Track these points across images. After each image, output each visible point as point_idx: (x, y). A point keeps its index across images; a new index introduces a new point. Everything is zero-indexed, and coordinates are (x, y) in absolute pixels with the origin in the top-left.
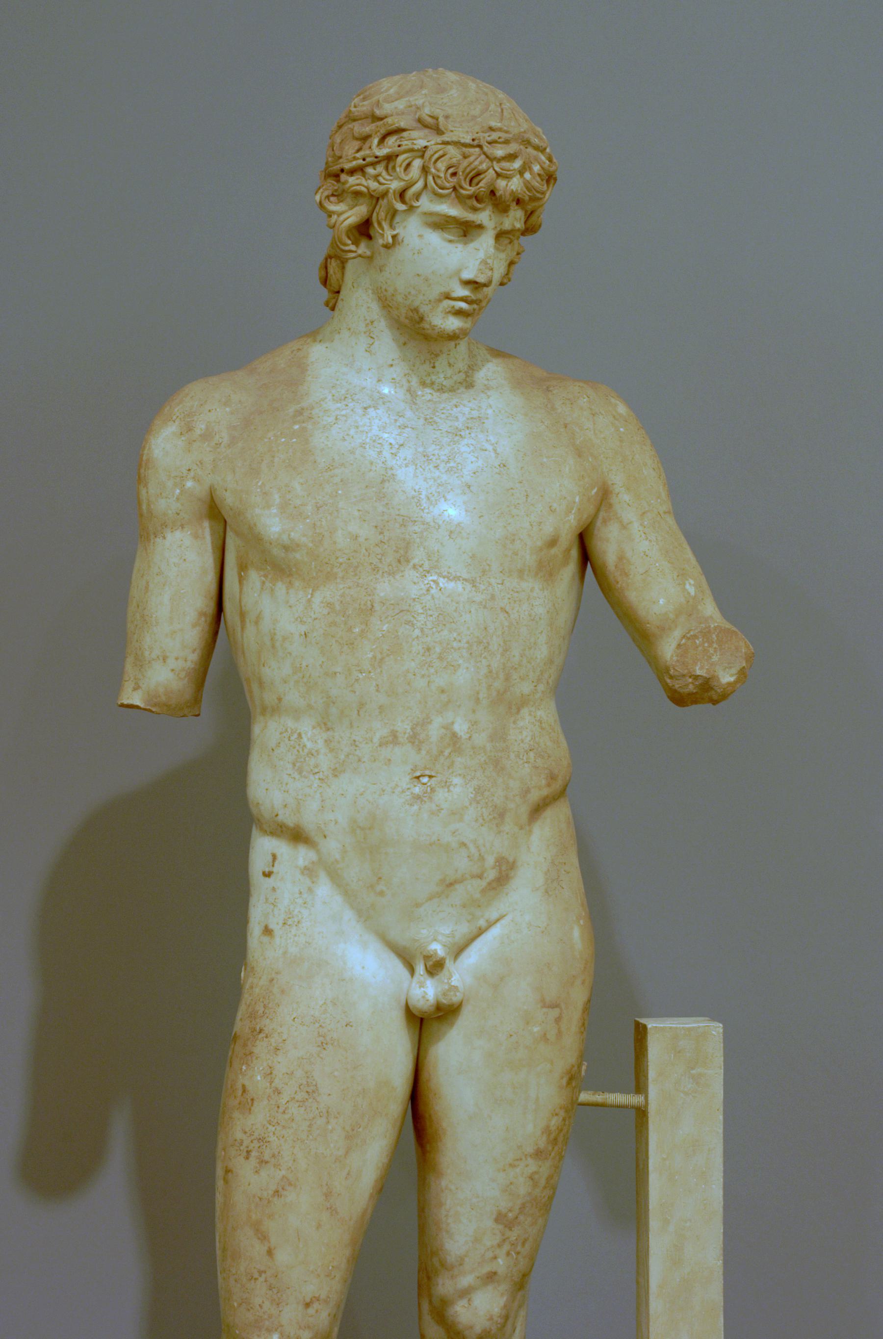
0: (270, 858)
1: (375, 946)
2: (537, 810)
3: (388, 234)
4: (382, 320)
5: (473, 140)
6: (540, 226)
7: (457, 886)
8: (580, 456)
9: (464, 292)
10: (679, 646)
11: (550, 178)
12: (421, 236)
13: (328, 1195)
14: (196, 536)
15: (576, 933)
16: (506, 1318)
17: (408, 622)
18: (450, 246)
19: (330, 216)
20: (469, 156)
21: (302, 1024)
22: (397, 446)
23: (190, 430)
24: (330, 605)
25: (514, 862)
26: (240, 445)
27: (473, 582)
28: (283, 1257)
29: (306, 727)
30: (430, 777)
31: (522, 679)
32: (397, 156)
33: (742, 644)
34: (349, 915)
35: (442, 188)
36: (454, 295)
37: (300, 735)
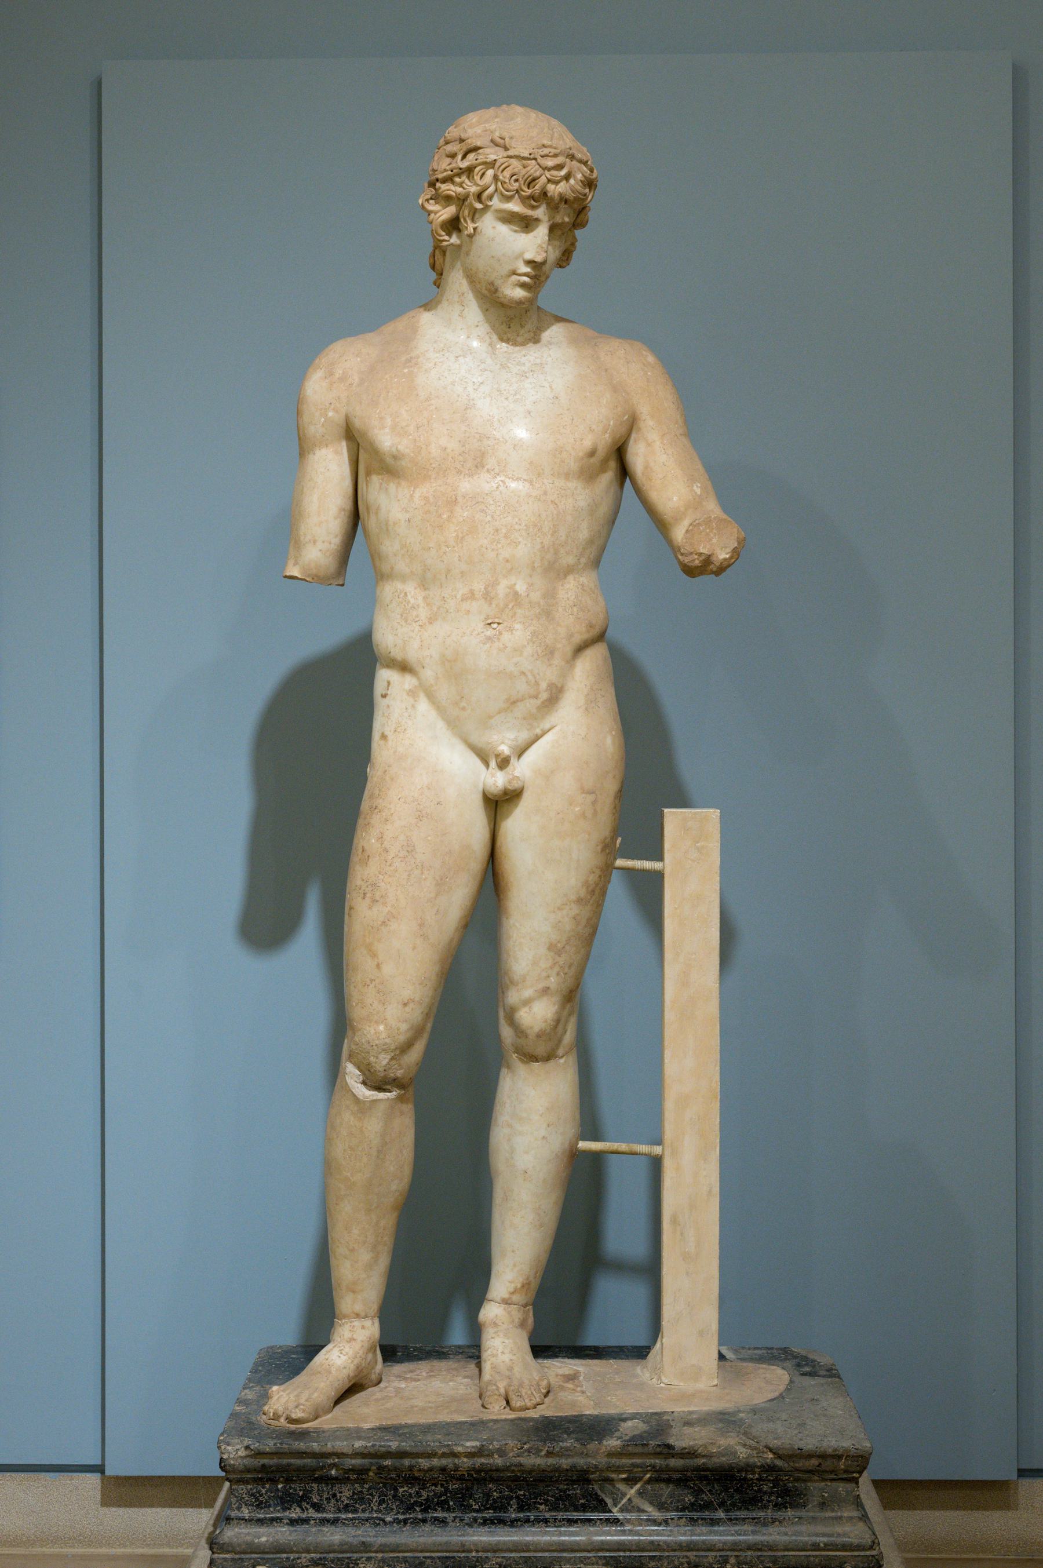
0: (386, 684)
1: (461, 748)
2: (580, 649)
3: (471, 226)
7: (519, 704)
8: (615, 392)
9: (528, 270)
10: (687, 531)
12: (494, 228)
13: (421, 925)
14: (336, 452)
15: (609, 741)
16: (558, 1021)
17: (482, 511)
21: (405, 802)
23: (332, 374)
24: (426, 498)
25: (562, 687)
27: (531, 482)
28: (388, 969)
29: (411, 589)
30: (499, 624)
31: (567, 553)
33: (735, 530)
34: (441, 724)
36: (519, 271)
37: (406, 594)
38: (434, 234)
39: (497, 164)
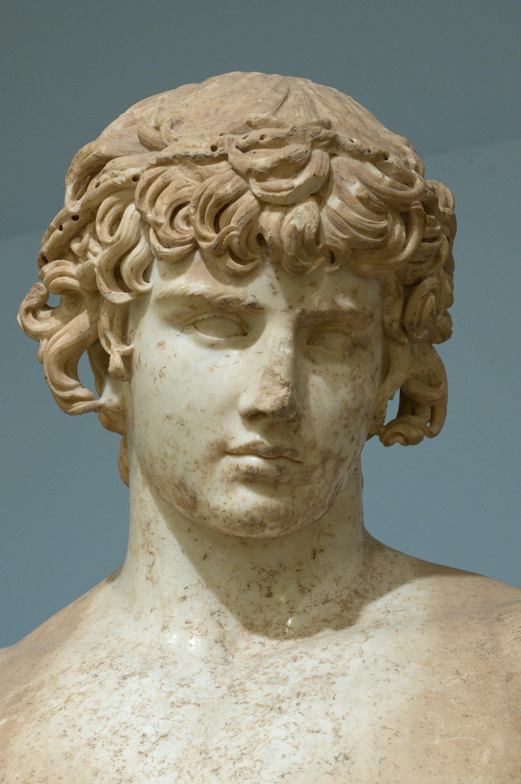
4: (161, 518)
5: (214, 148)
22: (154, 739)
36: (234, 444)
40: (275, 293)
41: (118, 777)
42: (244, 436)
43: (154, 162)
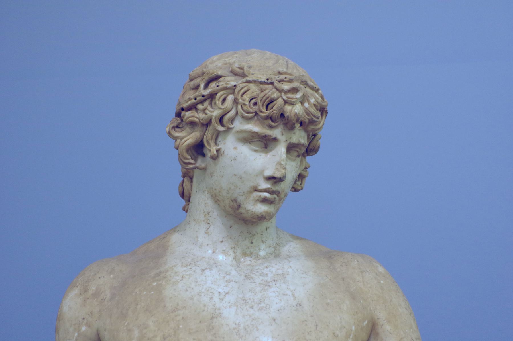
5: (267, 80)
6: (319, 147)
11: (323, 110)
12: (235, 148)
18: (257, 155)
19: (176, 141)
20: (265, 90)
22: (224, 294)
23: (86, 290)
26: (117, 298)
32: (217, 94)
35: (248, 113)
36: (260, 188)
38: (181, 158)
39: (237, 89)
40: (283, 135)
41: (213, 307)
42: (265, 185)
43: (245, 81)
